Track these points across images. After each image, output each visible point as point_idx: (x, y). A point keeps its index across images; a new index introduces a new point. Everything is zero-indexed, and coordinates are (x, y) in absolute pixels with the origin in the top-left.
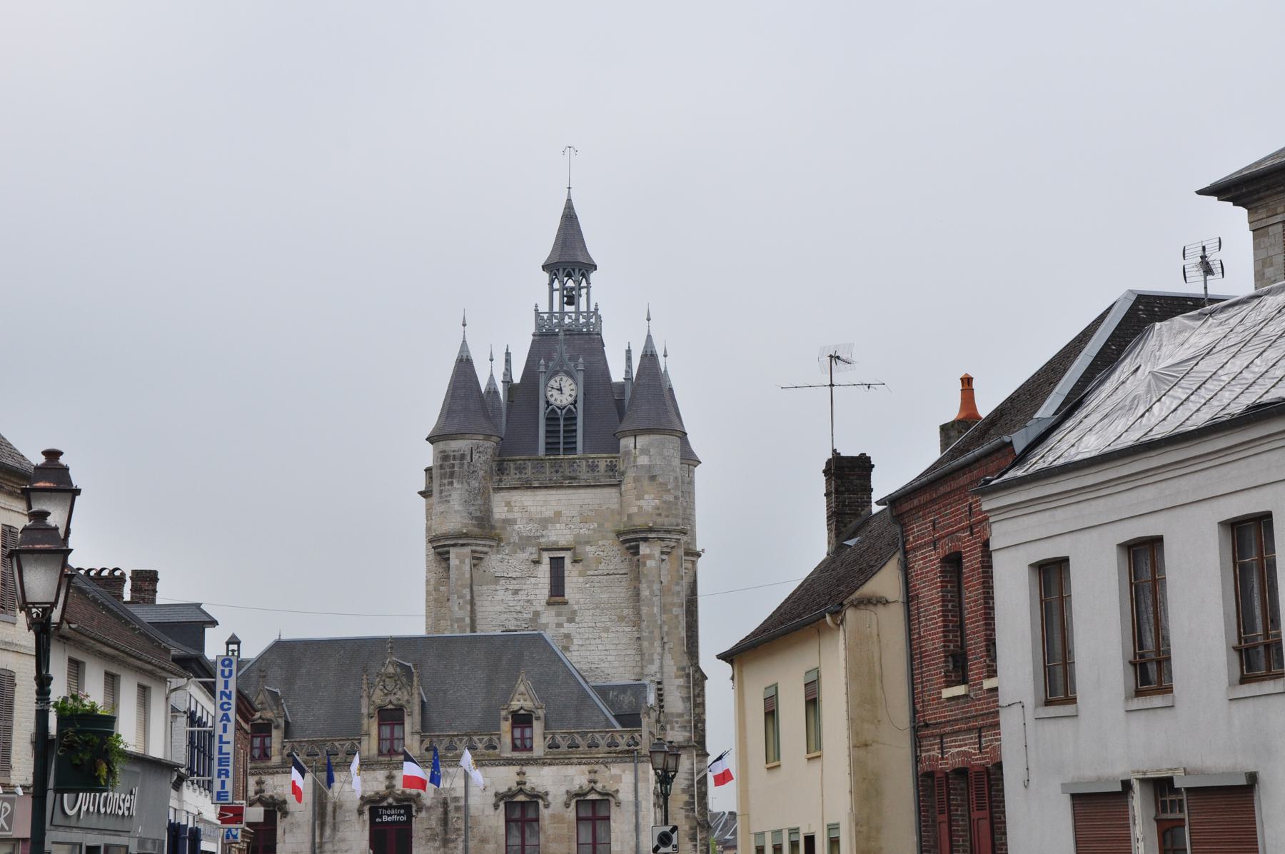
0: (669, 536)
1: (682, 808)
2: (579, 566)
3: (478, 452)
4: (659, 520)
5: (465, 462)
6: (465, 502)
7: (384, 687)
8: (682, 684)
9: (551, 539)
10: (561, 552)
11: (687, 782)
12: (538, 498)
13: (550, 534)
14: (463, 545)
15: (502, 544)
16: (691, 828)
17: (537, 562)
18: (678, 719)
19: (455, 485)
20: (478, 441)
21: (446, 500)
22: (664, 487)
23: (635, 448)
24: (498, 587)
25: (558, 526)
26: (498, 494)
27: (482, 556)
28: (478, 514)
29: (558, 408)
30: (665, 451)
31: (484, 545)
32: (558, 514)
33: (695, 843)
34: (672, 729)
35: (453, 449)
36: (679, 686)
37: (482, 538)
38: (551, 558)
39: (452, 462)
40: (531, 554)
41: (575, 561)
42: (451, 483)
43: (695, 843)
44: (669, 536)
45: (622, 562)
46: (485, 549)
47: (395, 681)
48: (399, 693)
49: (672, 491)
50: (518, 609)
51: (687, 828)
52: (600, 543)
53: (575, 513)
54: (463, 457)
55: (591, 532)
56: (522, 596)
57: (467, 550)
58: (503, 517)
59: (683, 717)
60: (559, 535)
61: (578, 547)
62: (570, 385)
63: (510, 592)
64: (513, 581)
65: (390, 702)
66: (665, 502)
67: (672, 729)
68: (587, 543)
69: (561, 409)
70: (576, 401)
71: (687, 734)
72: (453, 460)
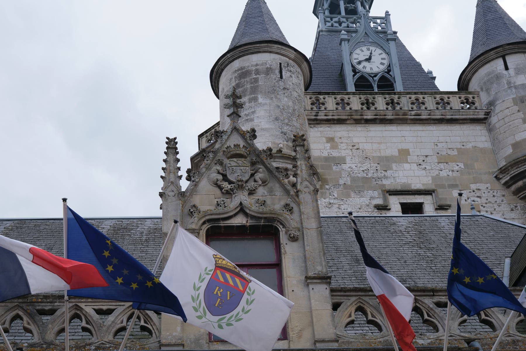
7: (225, 178)
9: (398, 181)
10: (417, 196)
12: (371, 134)
13: (397, 175)
15: (327, 187)
19: (260, 100)
20: (288, 59)
21: (247, 120)
23: (507, 68)
25: (406, 166)
26: (316, 129)
29: (369, 74)
35: (255, 63)
38: (402, 205)
39: (255, 77)
40: (372, 198)
42: (255, 99)
45: (512, 210)
47: (253, 164)
48: (261, 191)
52: (473, 187)
53: (429, 152)
54: (269, 71)
55: (455, 174)
58: (325, 154)
61: (439, 190)
62: (380, 54)
65: (242, 210)
70: (389, 71)
72: (256, 75)
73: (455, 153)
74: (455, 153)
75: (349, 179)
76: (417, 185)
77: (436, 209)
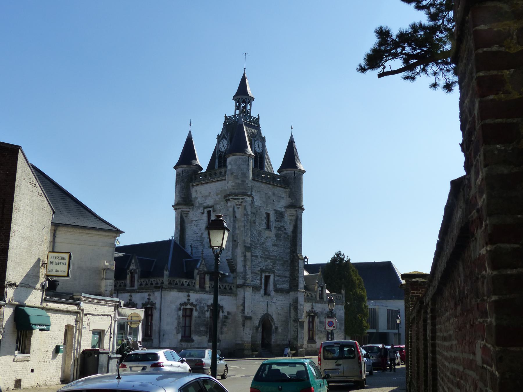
0: (237, 197)
1: (240, 312)
2: (215, 213)
3: (185, 172)
4: (233, 191)
5: (180, 176)
6: (179, 192)
8: (243, 259)
10: (210, 208)
11: (243, 301)
14: (179, 209)
16: (244, 321)
17: (203, 213)
18: (241, 275)
22: (236, 178)
24: (192, 224)
27: (187, 212)
28: (183, 196)
30: (237, 162)
31: (186, 208)
32: (210, 193)
33: (244, 327)
34: (239, 279)
36: (242, 261)
37: (185, 205)
38: (207, 211)
41: (214, 211)
43: (244, 327)
44: (237, 197)
46: (188, 210)
49: (240, 179)
50: (197, 232)
51: (241, 320)
52: (221, 203)
56: (198, 227)
57: (180, 210)
59: (242, 273)
60: (210, 202)
61: (215, 206)
63: (195, 226)
64: (196, 222)
66: (236, 183)
67: (239, 279)
68: (217, 204)
69: (222, 152)
71: (244, 281)
73: (219, 192)
74: (219, 192)
75: (198, 204)
76: (210, 205)
77: (213, 212)
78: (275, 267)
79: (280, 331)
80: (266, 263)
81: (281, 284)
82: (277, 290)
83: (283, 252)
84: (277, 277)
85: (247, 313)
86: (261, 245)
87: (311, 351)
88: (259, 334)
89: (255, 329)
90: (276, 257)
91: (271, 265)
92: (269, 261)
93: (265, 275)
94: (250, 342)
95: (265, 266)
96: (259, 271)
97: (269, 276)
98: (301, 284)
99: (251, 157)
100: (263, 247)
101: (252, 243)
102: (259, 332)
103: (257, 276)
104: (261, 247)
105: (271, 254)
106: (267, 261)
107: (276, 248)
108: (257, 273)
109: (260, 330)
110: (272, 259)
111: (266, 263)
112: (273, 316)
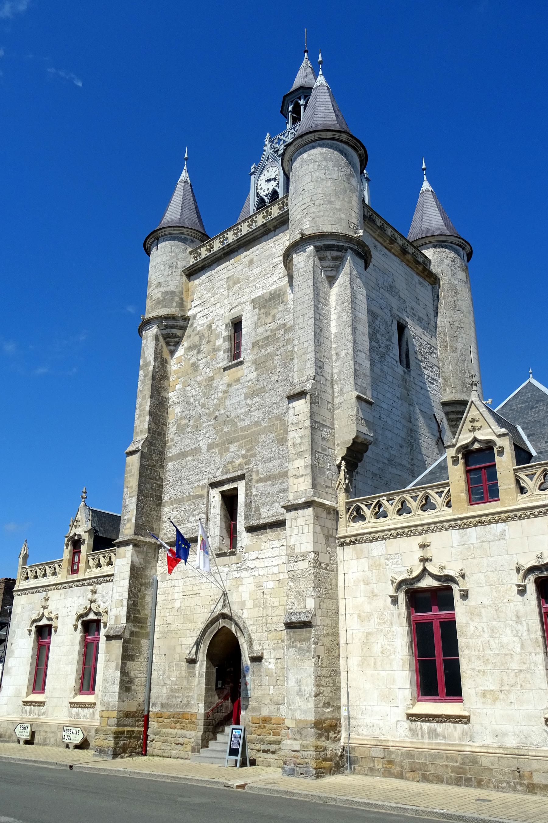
78: (255, 454)
79: (272, 666)
80: (228, 457)
81: (273, 502)
82: (251, 529)
83: (281, 400)
84: (261, 484)
85: (116, 617)
86: (209, 415)
87: (435, 757)
88: (197, 680)
89: (184, 664)
90: (256, 424)
91: (243, 456)
92: (233, 447)
93: (222, 493)
94: (114, 706)
95: (222, 466)
96: (203, 487)
97: (236, 489)
98: (301, 479)
99: (160, 235)
100: (216, 417)
101: (187, 421)
102: (197, 672)
103: (198, 504)
104: (210, 421)
105: (240, 424)
106: (227, 450)
107: (257, 399)
108: (196, 497)
109: (201, 666)
110: (244, 437)
111: (228, 457)
112: (245, 616)
